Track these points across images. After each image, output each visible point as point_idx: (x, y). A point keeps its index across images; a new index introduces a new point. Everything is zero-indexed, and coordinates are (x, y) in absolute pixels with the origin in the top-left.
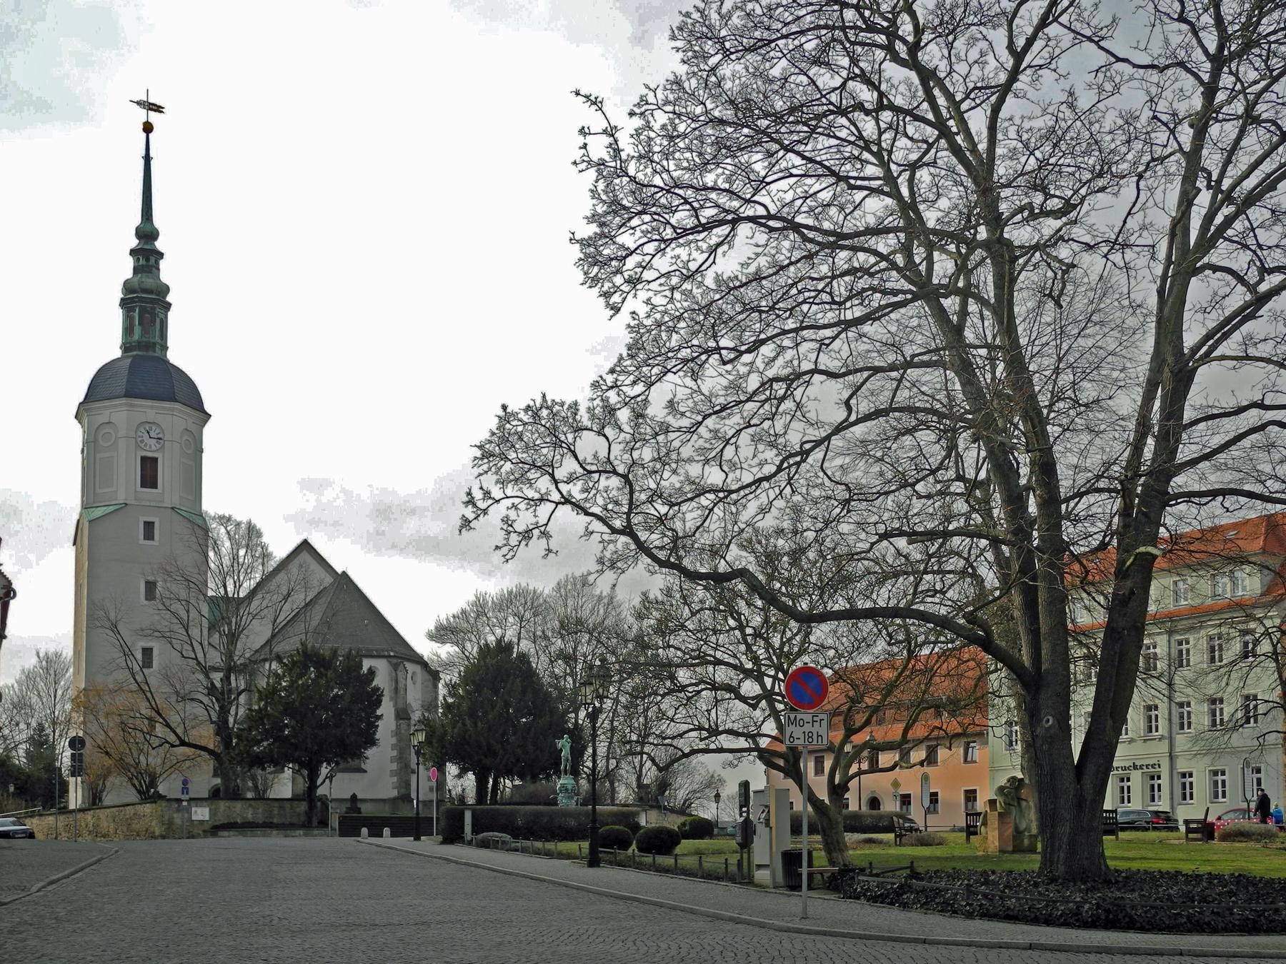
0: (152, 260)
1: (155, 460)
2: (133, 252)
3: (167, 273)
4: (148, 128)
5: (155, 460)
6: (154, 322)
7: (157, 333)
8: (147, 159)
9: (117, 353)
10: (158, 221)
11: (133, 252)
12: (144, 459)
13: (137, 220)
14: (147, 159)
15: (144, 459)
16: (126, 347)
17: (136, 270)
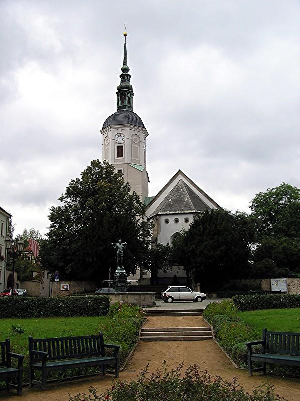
0: (126, 77)
1: (122, 147)
2: (120, 76)
3: (132, 82)
4: (125, 35)
5: (122, 147)
6: (125, 98)
7: (127, 102)
8: (125, 44)
9: (115, 110)
10: (129, 65)
11: (120, 76)
12: (118, 147)
13: (122, 65)
14: (125, 44)
15: (118, 147)
16: (118, 109)
17: (122, 82)
